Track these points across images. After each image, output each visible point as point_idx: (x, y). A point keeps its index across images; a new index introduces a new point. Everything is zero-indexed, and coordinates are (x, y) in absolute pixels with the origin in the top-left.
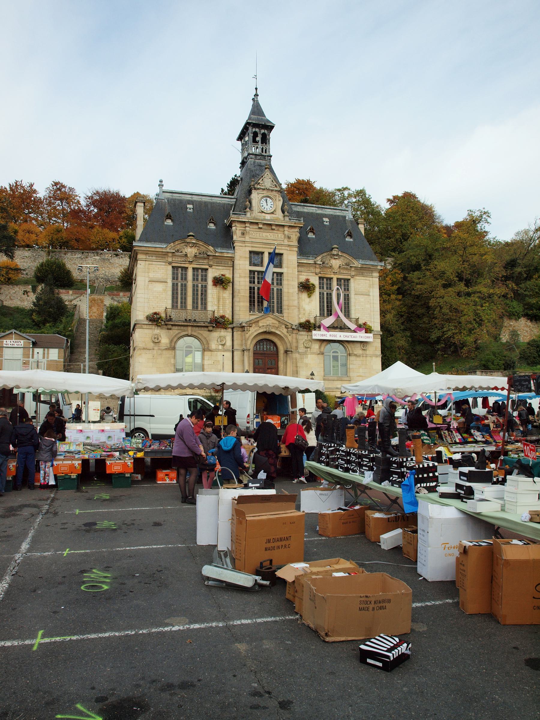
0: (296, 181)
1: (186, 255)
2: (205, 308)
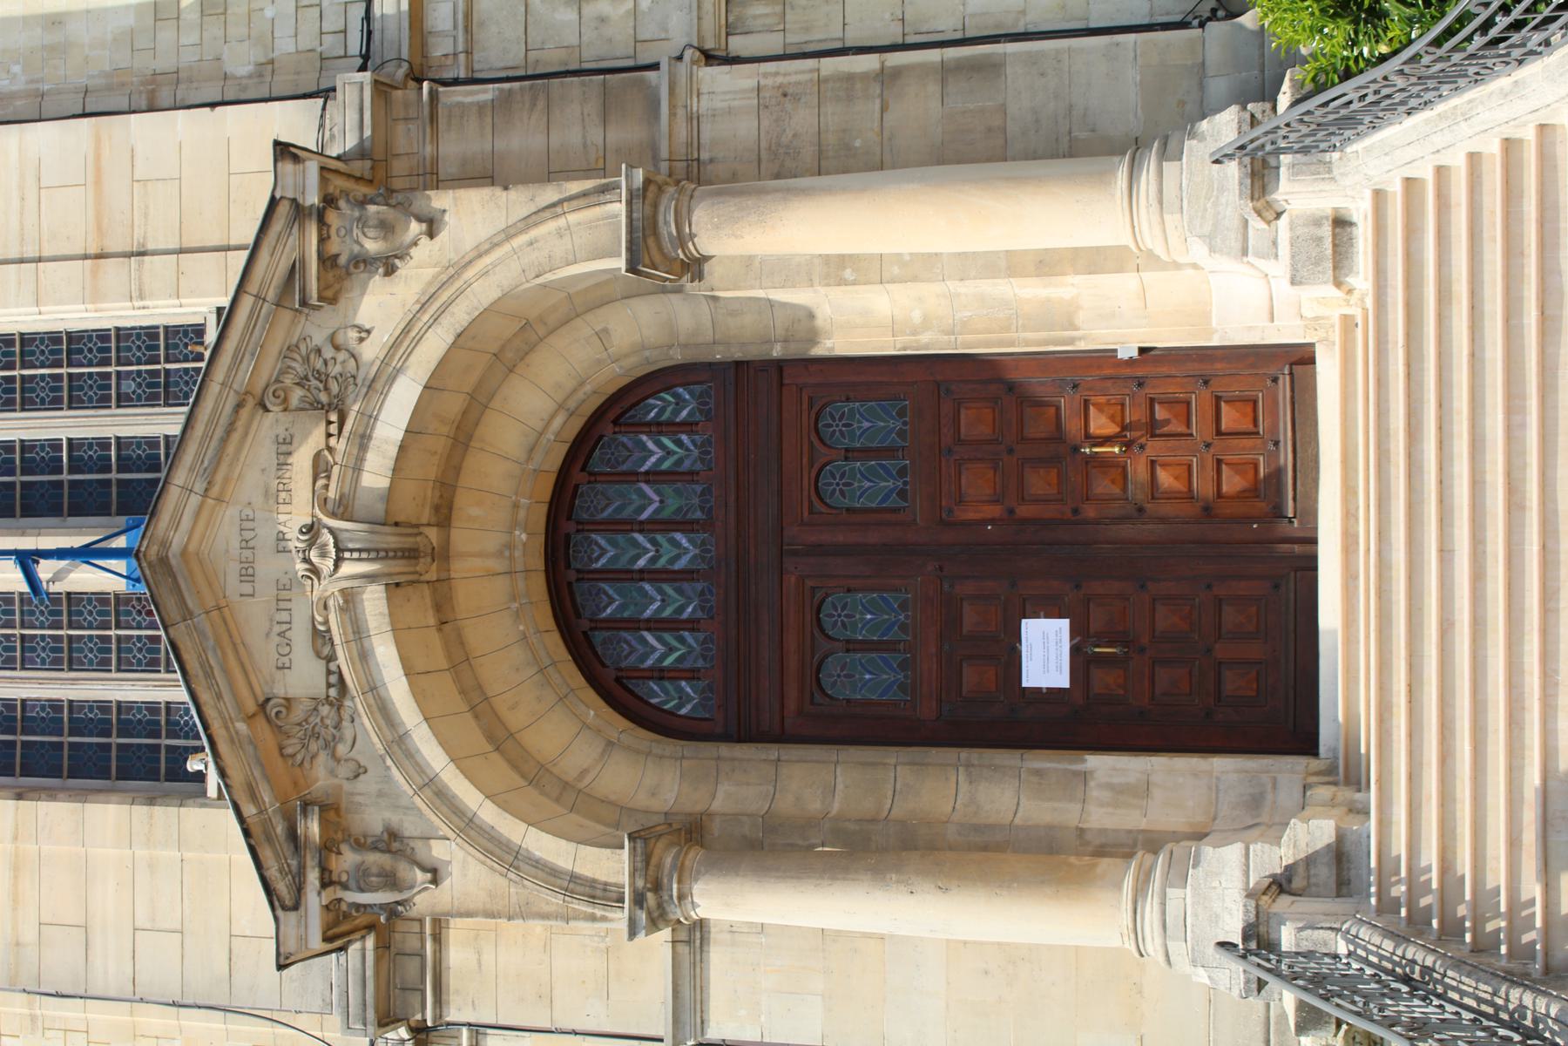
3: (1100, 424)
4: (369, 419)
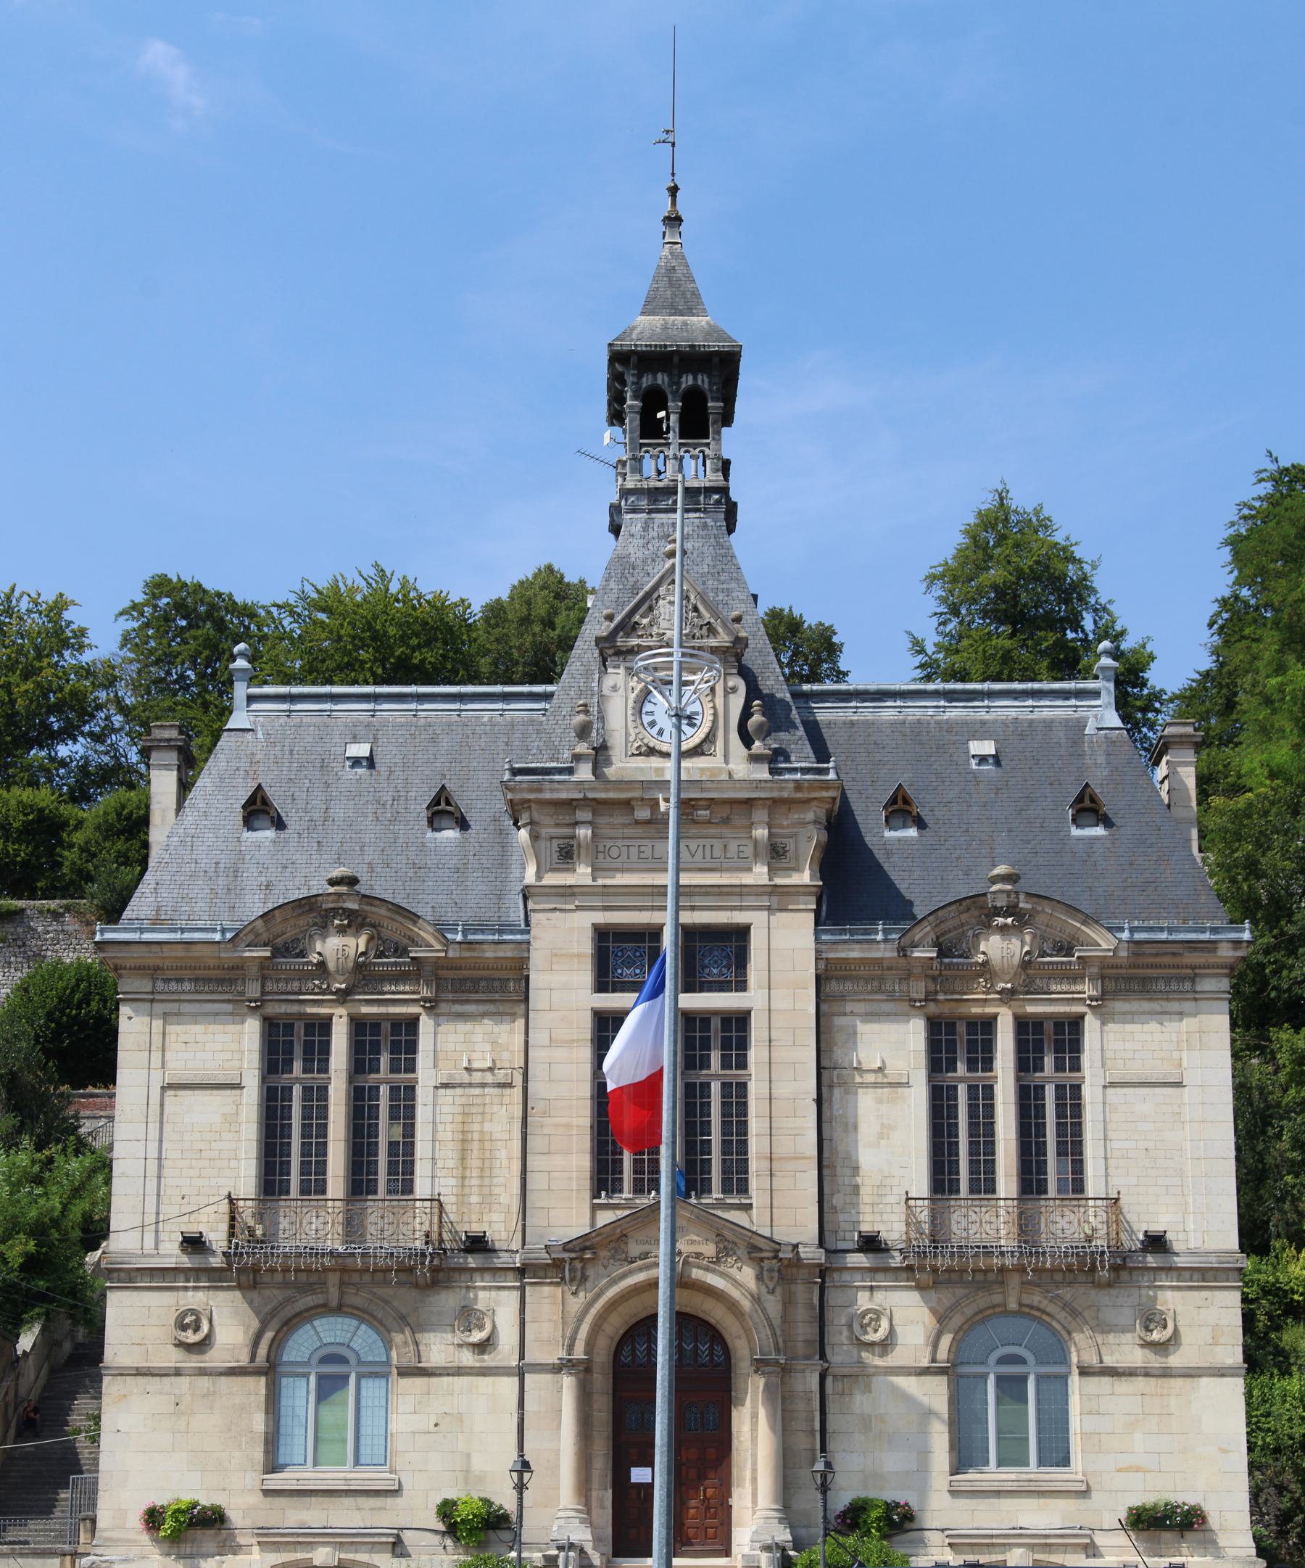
0: (787, 611)
1: (322, 965)
2: (408, 1188)
3: (710, 1492)
4: (713, 1271)
